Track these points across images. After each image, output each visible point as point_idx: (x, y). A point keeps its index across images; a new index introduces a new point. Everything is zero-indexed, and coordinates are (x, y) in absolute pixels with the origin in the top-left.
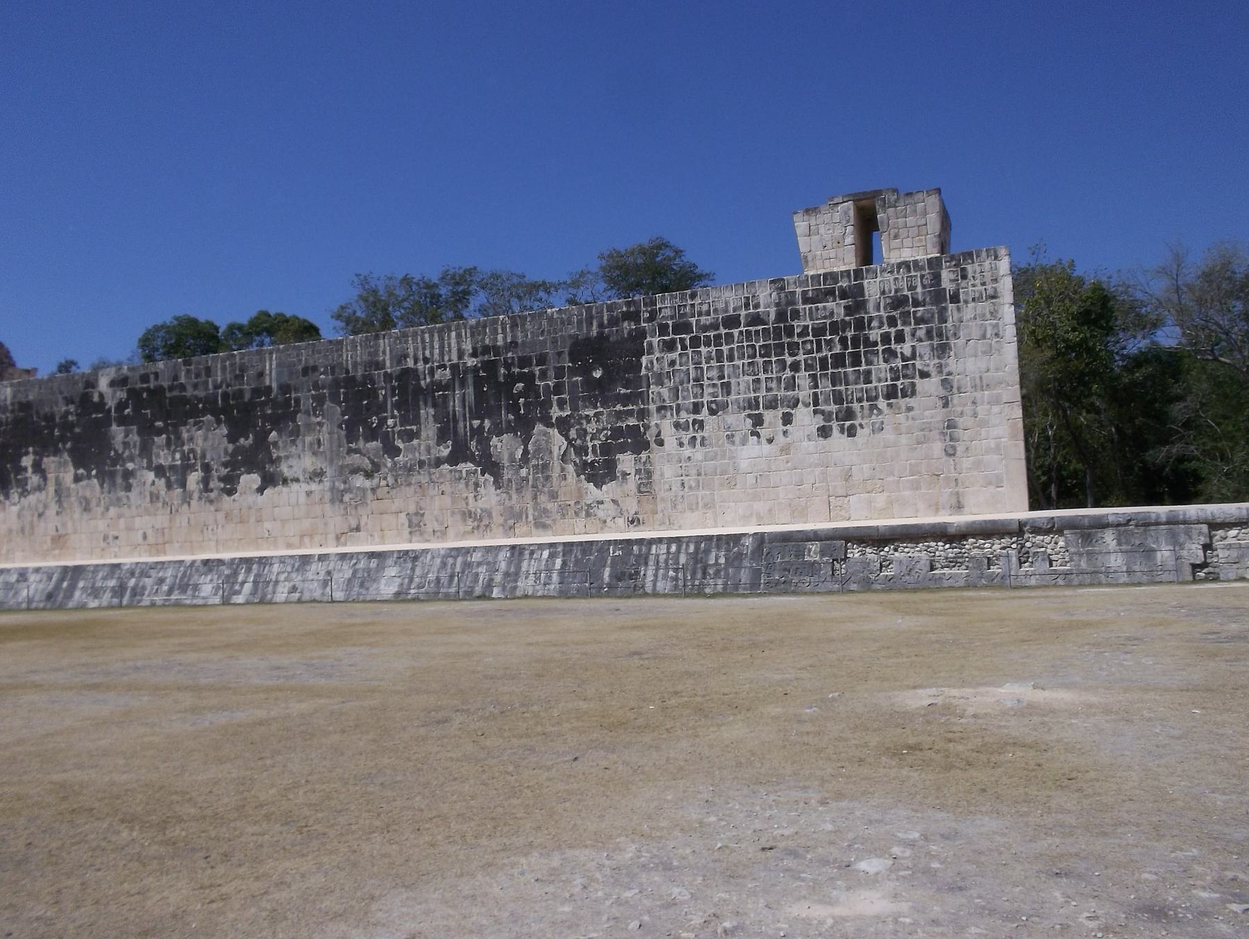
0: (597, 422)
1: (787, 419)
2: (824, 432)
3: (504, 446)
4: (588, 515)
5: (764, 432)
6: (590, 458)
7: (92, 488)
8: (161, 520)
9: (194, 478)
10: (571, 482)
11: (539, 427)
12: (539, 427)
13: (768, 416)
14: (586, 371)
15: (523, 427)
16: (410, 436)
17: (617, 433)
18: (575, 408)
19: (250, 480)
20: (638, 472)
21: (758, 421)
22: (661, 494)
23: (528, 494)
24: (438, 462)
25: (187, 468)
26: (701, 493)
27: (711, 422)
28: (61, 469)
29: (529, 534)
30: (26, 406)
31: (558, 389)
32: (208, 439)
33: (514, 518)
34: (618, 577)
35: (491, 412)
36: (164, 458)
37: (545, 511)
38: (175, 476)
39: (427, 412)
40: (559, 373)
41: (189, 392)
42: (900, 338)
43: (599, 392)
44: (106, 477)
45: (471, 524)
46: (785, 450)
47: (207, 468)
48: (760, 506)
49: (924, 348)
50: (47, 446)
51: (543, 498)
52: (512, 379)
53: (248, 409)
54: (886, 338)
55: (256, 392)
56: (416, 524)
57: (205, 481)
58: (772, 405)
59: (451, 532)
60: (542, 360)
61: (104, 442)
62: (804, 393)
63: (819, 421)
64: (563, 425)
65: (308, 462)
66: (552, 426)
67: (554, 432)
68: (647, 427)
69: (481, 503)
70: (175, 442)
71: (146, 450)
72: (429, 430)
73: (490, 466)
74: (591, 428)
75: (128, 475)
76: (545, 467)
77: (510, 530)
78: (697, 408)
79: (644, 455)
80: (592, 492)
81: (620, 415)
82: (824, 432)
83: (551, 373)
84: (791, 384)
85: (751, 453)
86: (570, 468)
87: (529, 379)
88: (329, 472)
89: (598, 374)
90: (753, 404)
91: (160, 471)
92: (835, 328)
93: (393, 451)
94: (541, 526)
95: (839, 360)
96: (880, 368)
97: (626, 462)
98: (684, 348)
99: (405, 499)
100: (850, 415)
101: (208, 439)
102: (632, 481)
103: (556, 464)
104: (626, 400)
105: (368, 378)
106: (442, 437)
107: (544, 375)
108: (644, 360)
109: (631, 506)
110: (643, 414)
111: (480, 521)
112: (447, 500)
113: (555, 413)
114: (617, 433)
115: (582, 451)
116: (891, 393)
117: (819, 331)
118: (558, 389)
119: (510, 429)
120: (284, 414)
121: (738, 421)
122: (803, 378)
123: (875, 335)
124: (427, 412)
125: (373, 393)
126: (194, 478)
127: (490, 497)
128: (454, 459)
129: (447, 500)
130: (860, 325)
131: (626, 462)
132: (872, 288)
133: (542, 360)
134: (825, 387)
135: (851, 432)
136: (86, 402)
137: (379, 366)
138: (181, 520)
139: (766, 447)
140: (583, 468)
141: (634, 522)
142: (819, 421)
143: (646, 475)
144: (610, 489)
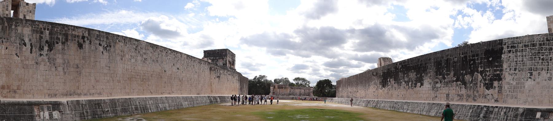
0: (489, 72)
3: (468, 78)
4: (485, 98)
6: (487, 82)
7: (396, 85)
8: (405, 92)
9: (410, 83)
10: (482, 89)
11: (476, 73)
12: (476, 73)
14: (488, 59)
16: (448, 75)
17: (495, 75)
18: (484, 69)
20: (498, 87)
21: (531, 74)
22: (504, 94)
23: (472, 91)
24: (453, 81)
25: (410, 81)
26: (514, 94)
29: (471, 102)
31: (481, 63)
32: (413, 75)
33: (469, 96)
36: (406, 79)
37: (476, 96)
38: (407, 83)
40: (481, 59)
41: (411, 65)
43: (490, 64)
45: (459, 98)
47: (412, 82)
48: (530, 99)
51: (475, 92)
52: (470, 60)
55: (421, 65)
57: (412, 84)
58: (537, 69)
59: (455, 99)
60: (477, 55)
61: (398, 75)
64: (481, 73)
66: (478, 72)
67: (479, 75)
68: (502, 74)
69: (462, 93)
72: (452, 73)
73: (464, 83)
74: (488, 74)
75: (401, 82)
76: (477, 84)
77: (467, 100)
78: (515, 69)
79: (500, 82)
80: (487, 92)
81: (495, 71)
83: (479, 59)
86: (482, 85)
87: (474, 60)
88: (432, 83)
89: (490, 59)
93: (444, 78)
97: (496, 84)
98: (513, 52)
99: (445, 90)
102: (497, 89)
103: (479, 83)
104: (497, 66)
105: (441, 61)
106: (454, 76)
107: (478, 59)
108: (503, 56)
109: (496, 96)
111: (460, 97)
112: (454, 91)
113: (480, 69)
115: (485, 80)
118: (481, 63)
119: (469, 74)
125: (441, 64)
126: (410, 83)
127: (463, 91)
128: (457, 81)
129: (454, 91)
131: (496, 84)
133: (477, 55)
137: (443, 57)
138: (408, 92)
139: (533, 82)
140: (485, 84)
141: (496, 101)
143: (500, 87)
144: (491, 91)
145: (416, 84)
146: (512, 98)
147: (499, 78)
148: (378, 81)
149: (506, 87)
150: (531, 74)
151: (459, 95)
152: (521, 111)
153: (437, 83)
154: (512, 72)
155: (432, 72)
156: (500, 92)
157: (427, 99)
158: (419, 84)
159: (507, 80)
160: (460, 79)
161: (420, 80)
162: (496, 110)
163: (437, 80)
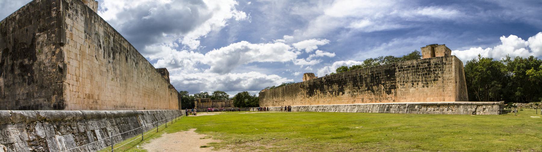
0: (388, 84)
1: (418, 84)
2: (423, 86)
3: (375, 88)
5: (414, 86)
7: (322, 94)
8: (330, 99)
9: (334, 93)
10: (384, 94)
13: (415, 83)
15: (377, 85)
17: (392, 86)
19: (341, 93)
21: (413, 84)
27: (406, 84)
28: (319, 92)
30: (314, 83)
32: (336, 87)
33: (377, 99)
34: (387, 110)
35: (373, 82)
36: (330, 90)
38: (331, 93)
39: (364, 82)
42: (436, 71)
44: (323, 93)
46: (417, 89)
48: (413, 99)
49: (440, 72)
50: (317, 89)
53: (341, 82)
54: (434, 70)
56: (363, 101)
58: (415, 82)
61: (323, 87)
62: (420, 80)
63: (423, 84)
64: (383, 84)
65: (348, 90)
70: (332, 87)
71: (328, 89)
72: (364, 85)
73: (373, 91)
74: (388, 85)
77: (376, 102)
80: (388, 96)
81: (392, 83)
82: (423, 86)
84: (419, 78)
85: (412, 90)
90: (412, 81)
91: (330, 92)
92: (426, 68)
93: (359, 89)
94: (380, 101)
95: (426, 74)
96: (433, 76)
97: (393, 91)
99: (360, 96)
100: (428, 84)
101: (336, 87)
102: (394, 94)
104: (393, 80)
106: (366, 86)
109: (393, 98)
110: (395, 83)
111: (371, 100)
113: (382, 82)
114: (392, 86)
115: (386, 89)
116: (434, 80)
117: (423, 69)
120: (345, 83)
121: (410, 84)
122: (420, 77)
123: (432, 70)
124: (364, 82)
126: (334, 93)
127: (373, 96)
128: (368, 90)
130: (430, 68)
131: (393, 91)
132: (432, 61)
134: (424, 79)
135: (428, 87)
136: (321, 82)
140: (386, 92)
141: (394, 101)
142: (423, 84)
145: (338, 93)
146: (403, 99)
147: (395, 87)
148: (304, 92)
149: (399, 92)
150: (413, 84)
151: (370, 99)
152: (407, 105)
153: (355, 92)
154: (402, 83)
155: (350, 85)
156: (396, 95)
157: (348, 102)
158: (341, 93)
159: (400, 88)
160: (369, 88)
161: (342, 90)
162: (394, 106)
163: (354, 90)
